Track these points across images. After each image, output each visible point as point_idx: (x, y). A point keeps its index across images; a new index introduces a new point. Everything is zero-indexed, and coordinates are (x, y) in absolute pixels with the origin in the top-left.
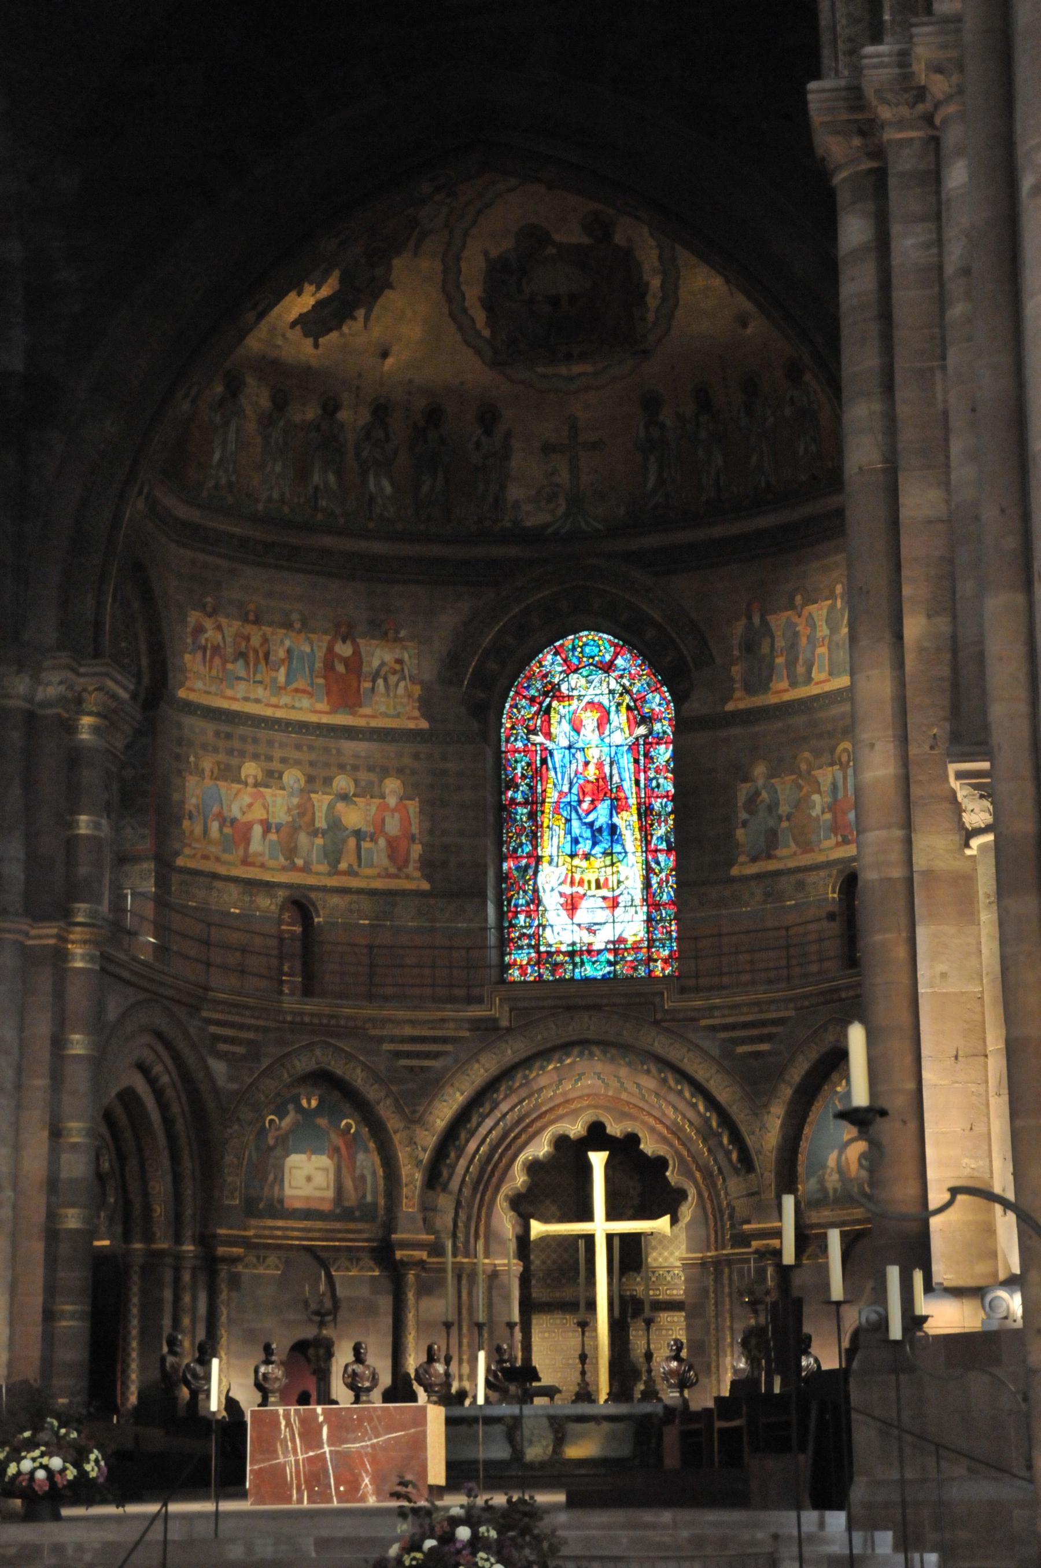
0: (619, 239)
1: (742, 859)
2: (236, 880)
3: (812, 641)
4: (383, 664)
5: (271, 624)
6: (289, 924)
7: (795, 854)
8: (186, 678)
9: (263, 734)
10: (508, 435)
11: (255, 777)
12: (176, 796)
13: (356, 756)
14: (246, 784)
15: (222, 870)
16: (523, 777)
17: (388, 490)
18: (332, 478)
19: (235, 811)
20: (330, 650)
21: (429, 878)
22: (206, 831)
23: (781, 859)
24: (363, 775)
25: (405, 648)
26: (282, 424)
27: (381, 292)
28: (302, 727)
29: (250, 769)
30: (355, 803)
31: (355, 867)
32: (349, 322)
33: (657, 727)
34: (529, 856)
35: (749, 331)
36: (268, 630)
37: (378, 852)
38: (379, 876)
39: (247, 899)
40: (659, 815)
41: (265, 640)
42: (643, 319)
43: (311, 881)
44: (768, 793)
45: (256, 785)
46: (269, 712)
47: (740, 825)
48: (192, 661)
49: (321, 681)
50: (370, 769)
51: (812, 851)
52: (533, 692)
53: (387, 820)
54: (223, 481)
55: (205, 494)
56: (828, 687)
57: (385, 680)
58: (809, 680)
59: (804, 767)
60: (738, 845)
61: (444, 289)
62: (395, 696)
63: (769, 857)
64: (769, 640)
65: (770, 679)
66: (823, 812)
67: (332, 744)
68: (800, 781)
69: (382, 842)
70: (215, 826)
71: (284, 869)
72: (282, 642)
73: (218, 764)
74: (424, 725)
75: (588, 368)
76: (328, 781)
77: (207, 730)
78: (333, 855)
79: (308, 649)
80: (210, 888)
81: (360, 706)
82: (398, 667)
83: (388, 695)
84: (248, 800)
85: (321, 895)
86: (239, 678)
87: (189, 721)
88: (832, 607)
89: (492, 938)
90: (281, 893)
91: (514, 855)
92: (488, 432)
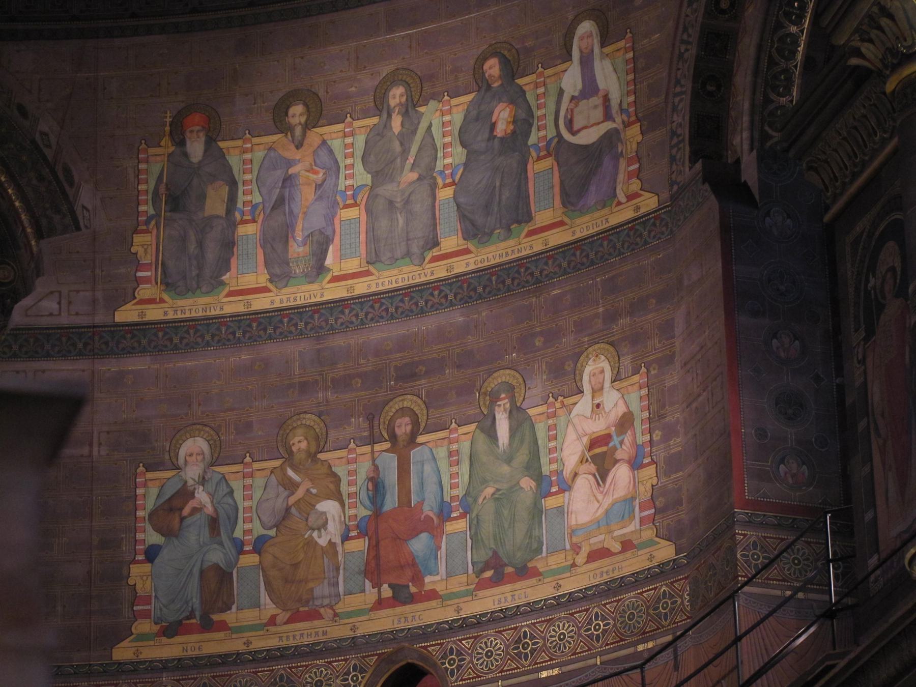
1: (143, 626)
7: (272, 621)
44: (212, 496)
47: (140, 557)
51: (314, 615)
56: (361, 287)
58: (320, 269)
59: (300, 443)
60: (135, 598)
63: (207, 625)
65: (224, 265)
66: (346, 538)
68: (290, 473)
88: (377, 135)
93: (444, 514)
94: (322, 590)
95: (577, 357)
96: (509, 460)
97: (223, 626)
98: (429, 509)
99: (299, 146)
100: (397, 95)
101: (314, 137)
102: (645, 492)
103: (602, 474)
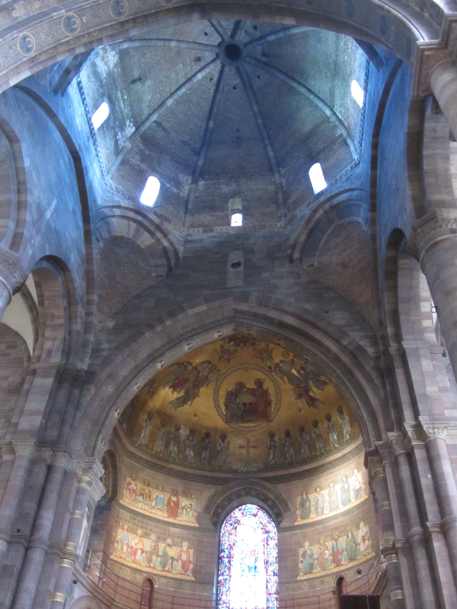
0: (265, 387)
1: (301, 574)
2: (129, 567)
3: (323, 502)
4: (186, 505)
5: (152, 487)
6: (146, 587)
7: (320, 571)
8: (123, 497)
9: (146, 521)
10: (229, 442)
11: (141, 534)
12: (114, 534)
13: (174, 533)
14: (138, 536)
15: (126, 563)
16: (227, 549)
17: (192, 454)
18: (176, 449)
19: (133, 544)
20: (170, 498)
21: (195, 577)
22: (122, 548)
23: (315, 573)
24: (176, 540)
25: (193, 501)
26: (163, 430)
27: (196, 397)
28: (158, 521)
29: (140, 531)
30: (173, 548)
31: (170, 570)
32: (186, 405)
33: (271, 535)
34: (228, 575)
35: (302, 413)
36: (151, 488)
37: (178, 566)
38: (178, 574)
39: (133, 574)
40: (271, 563)
41: (150, 492)
42: (270, 411)
43: (155, 572)
45: (141, 537)
46: (148, 514)
48: (126, 493)
49: (166, 507)
50: (178, 537)
51: (326, 570)
52: (231, 522)
53: (183, 555)
54: (143, 443)
55: (137, 445)
57: (186, 510)
58: (323, 513)
59: (322, 542)
60: (300, 569)
61: (214, 398)
62: (189, 515)
63: (310, 573)
64: (309, 503)
65: (309, 514)
66: (329, 556)
67: (167, 527)
69: (180, 562)
70: (125, 547)
71: (146, 566)
72: (155, 493)
73: (129, 527)
74: (197, 525)
75: (253, 424)
76: (164, 540)
77: (128, 515)
78: (164, 565)
79: (163, 497)
80: (121, 568)
81: (177, 517)
82: (190, 506)
83: (186, 515)
84: (137, 541)
85: (158, 577)
86: (140, 501)
87: (122, 511)
88: (330, 491)
89: (214, 596)
90: (144, 575)
91: (222, 574)
92: (223, 441)
93: (343, 551)
94: (326, 565)
95: (359, 523)
96: (351, 541)
97: (312, 573)
98: (341, 550)
99: (319, 494)
100: (332, 485)
101: (321, 493)
102: (370, 544)
103: (364, 542)
